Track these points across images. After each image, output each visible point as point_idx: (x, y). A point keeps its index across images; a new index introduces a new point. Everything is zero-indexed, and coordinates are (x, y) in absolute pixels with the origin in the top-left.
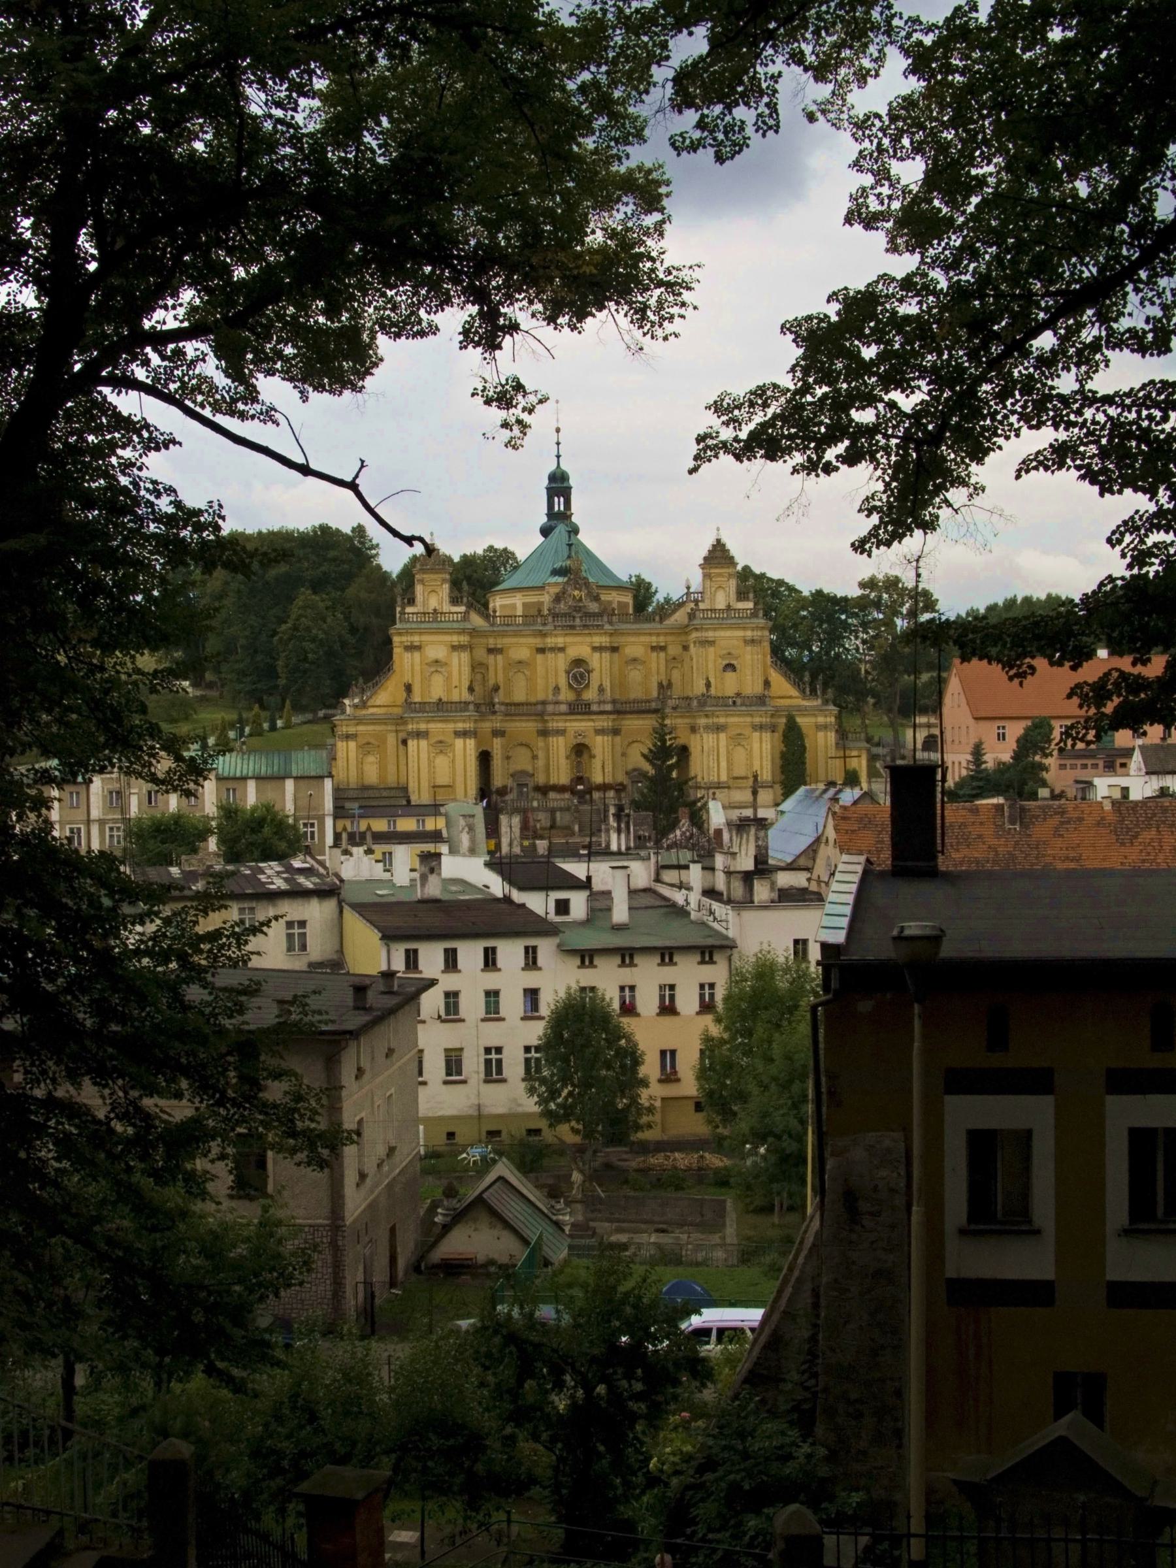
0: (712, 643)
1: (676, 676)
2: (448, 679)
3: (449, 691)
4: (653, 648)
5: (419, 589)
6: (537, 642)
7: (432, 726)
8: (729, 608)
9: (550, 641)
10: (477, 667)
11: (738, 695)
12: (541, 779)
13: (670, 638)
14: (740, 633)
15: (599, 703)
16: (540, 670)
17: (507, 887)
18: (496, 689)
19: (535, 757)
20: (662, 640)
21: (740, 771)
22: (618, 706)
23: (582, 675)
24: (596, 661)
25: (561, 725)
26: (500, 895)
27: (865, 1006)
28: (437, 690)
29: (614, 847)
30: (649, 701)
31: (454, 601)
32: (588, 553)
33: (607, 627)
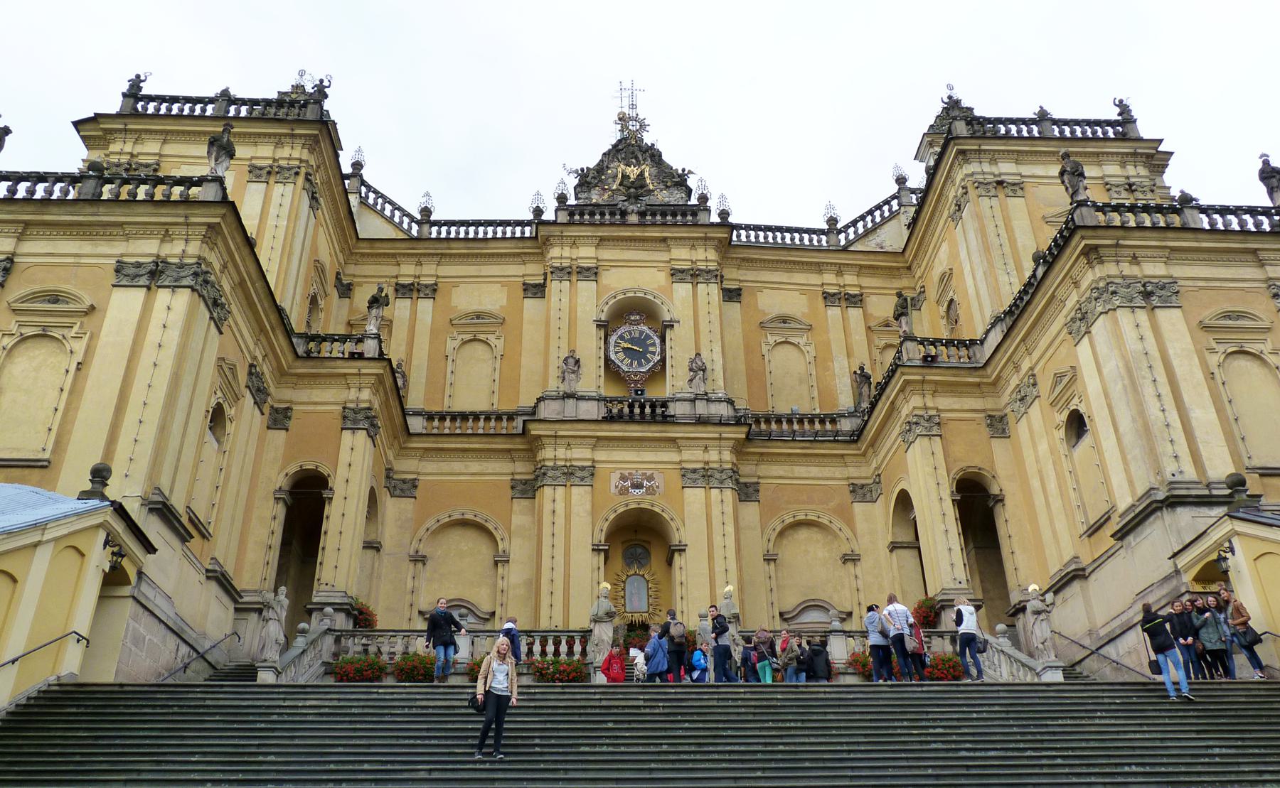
6: (532, 272)
9: (558, 254)
13: (867, 281)
19: (500, 560)
23: (642, 341)
25: (580, 454)
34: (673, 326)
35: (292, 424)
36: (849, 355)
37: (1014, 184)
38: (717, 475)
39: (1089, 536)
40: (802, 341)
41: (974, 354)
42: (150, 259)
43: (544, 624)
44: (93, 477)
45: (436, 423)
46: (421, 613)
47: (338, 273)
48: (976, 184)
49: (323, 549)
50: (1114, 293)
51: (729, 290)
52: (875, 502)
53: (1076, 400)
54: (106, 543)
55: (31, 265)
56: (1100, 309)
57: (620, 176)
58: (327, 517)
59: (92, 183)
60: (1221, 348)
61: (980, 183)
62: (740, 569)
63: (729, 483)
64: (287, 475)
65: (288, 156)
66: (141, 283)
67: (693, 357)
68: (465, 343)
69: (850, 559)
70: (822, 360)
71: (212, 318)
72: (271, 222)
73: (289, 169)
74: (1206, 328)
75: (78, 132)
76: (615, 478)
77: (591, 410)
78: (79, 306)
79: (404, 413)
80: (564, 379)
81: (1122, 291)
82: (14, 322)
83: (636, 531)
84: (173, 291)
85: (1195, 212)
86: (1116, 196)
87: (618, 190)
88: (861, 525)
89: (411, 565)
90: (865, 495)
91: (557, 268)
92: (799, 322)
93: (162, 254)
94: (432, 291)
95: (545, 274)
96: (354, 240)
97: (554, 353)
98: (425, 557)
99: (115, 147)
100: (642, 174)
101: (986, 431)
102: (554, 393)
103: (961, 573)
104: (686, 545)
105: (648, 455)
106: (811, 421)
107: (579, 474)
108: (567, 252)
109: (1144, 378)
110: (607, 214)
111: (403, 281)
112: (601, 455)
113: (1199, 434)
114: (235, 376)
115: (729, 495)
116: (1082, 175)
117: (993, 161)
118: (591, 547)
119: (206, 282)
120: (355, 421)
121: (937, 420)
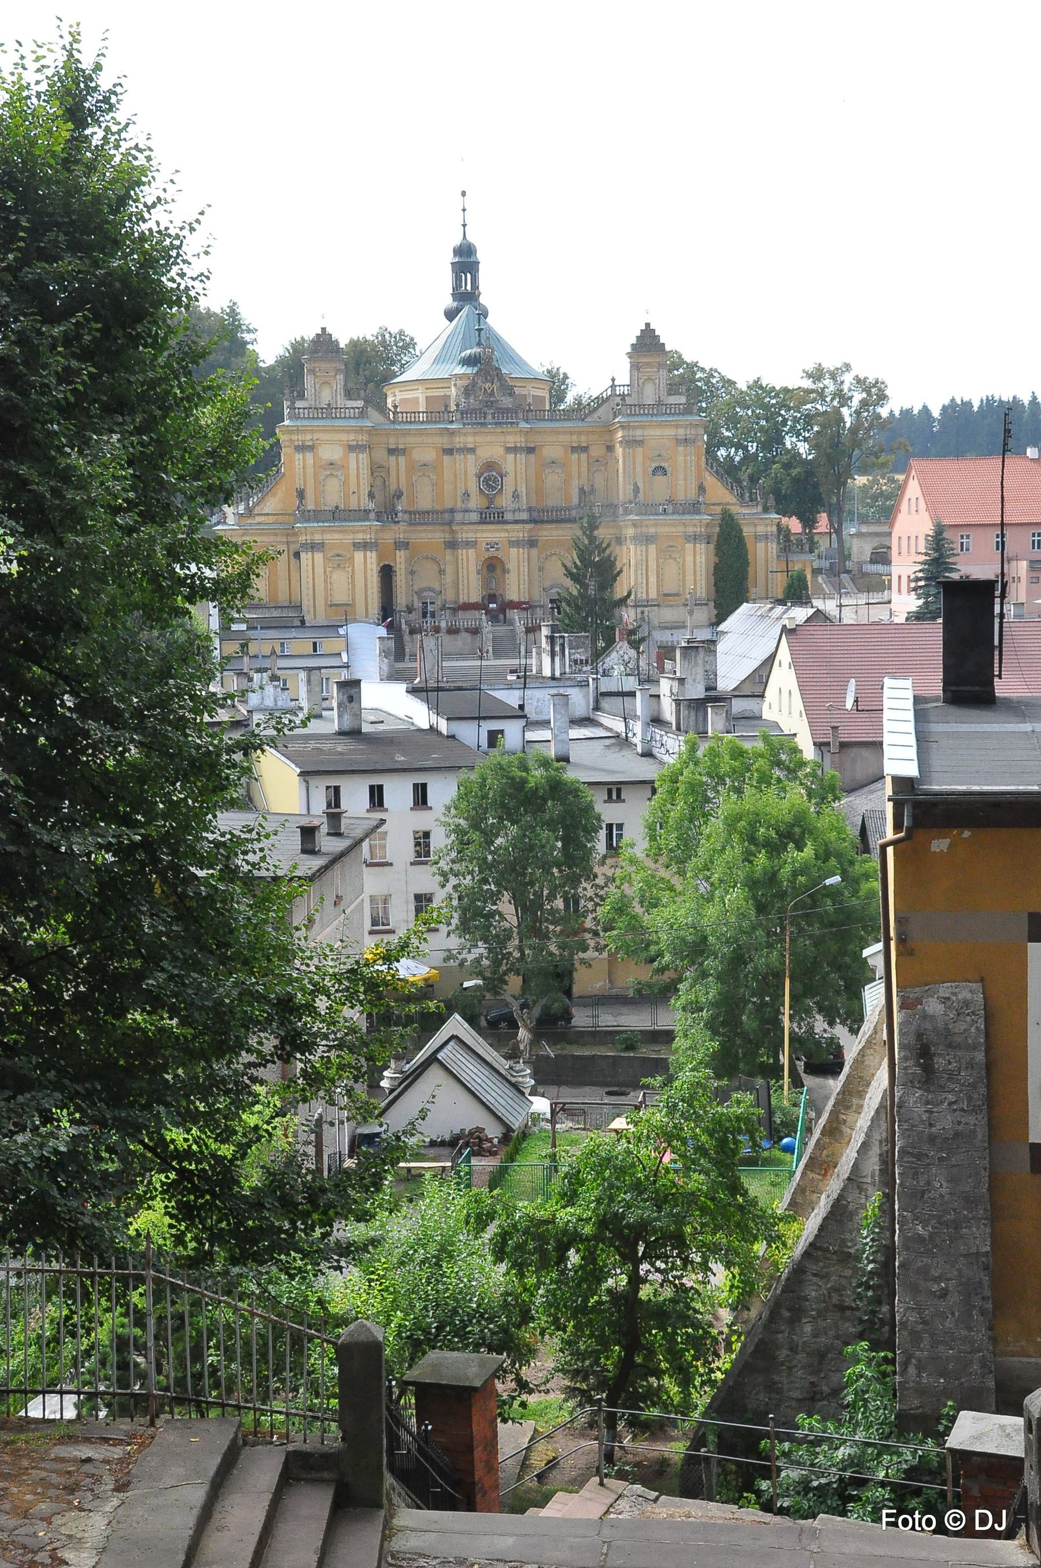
0: (641, 443)
1: (599, 480)
2: (345, 484)
3: (346, 497)
4: (574, 449)
5: (309, 381)
7: (327, 536)
8: (659, 403)
10: (375, 468)
11: (670, 501)
12: (449, 596)
14: (670, 432)
16: (448, 475)
17: (434, 718)
18: (399, 495)
19: (441, 572)
20: (584, 440)
21: (670, 587)
22: (535, 514)
24: (510, 464)
25: (471, 536)
26: (426, 726)
27: (940, 845)
28: (333, 496)
29: (547, 672)
30: (568, 509)
31: (349, 394)
32: (498, 339)
33: (523, 425)
36: (579, 477)
43: (461, 601)
62: (529, 580)
70: (567, 482)
72: (361, 471)
76: (484, 545)
94: (404, 452)
97: (459, 490)
105: (497, 535)
108: (462, 439)
111: (391, 447)
112: (479, 535)
117: (634, 428)
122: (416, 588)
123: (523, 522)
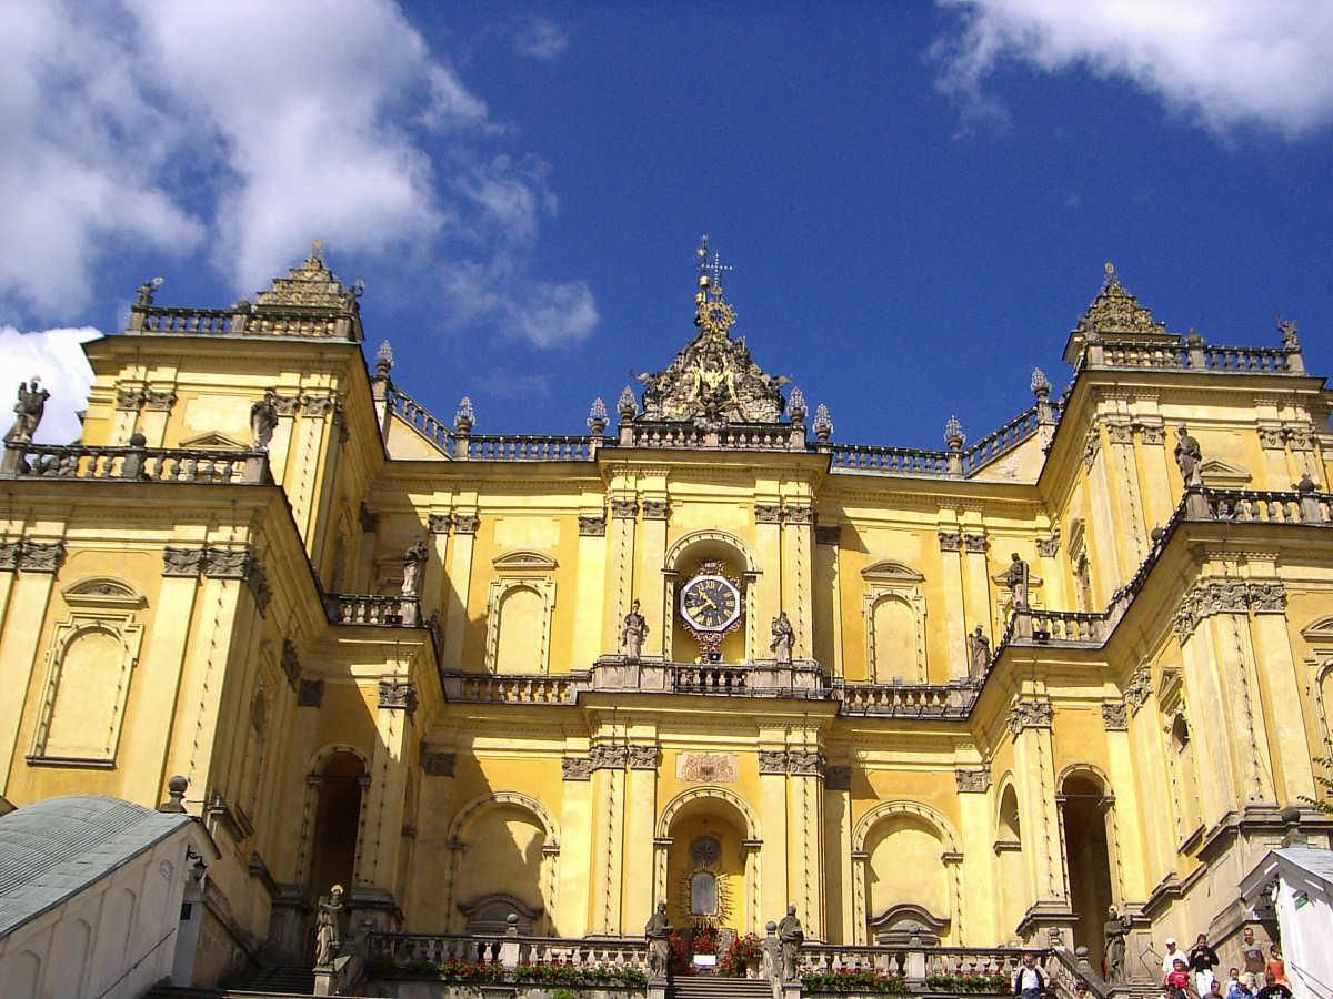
15: (775, 670)
34: (755, 577)
35: (325, 699)
37: (1154, 429)
38: (800, 760)
39: (1187, 853)
40: (911, 594)
41: (1096, 630)
42: (199, 547)
44: (172, 790)
45: (476, 688)
46: (462, 908)
47: (363, 504)
48: (1109, 428)
49: (361, 841)
50: (1216, 596)
51: (822, 529)
52: (985, 792)
53: (1181, 706)
54: (188, 854)
55: (78, 550)
56: (1200, 613)
57: (697, 383)
58: (365, 806)
59: (134, 457)
60: (1320, 660)
61: (1113, 426)
63: (812, 770)
64: (320, 757)
65: (316, 385)
66: (190, 573)
67: (778, 616)
68: (510, 591)
69: (952, 859)
71: (257, 605)
73: (318, 401)
74: (1309, 639)
75: (87, 354)
77: (656, 681)
78: (130, 597)
79: (442, 676)
80: (625, 642)
81: (1224, 594)
82: (68, 614)
83: (705, 821)
84: (224, 583)
85: (1311, 501)
86: (1270, 445)
87: (694, 402)
88: (966, 819)
89: (450, 857)
90: (973, 784)
91: (619, 503)
92: (908, 571)
93: (210, 540)
95: (605, 509)
96: (382, 462)
98: (463, 845)
99: (127, 373)
100: (723, 382)
101: (1100, 722)
102: (613, 658)
103: (1060, 884)
104: (762, 842)
106: (916, 694)
107: (641, 755)
109: (1235, 692)
110: (681, 434)
113: (1285, 756)
114: (274, 661)
115: (812, 781)
116: (1198, 457)
118: (653, 841)
119: (253, 570)
120: (395, 699)
121: (1047, 709)
122: (464, 894)
123: (806, 700)
